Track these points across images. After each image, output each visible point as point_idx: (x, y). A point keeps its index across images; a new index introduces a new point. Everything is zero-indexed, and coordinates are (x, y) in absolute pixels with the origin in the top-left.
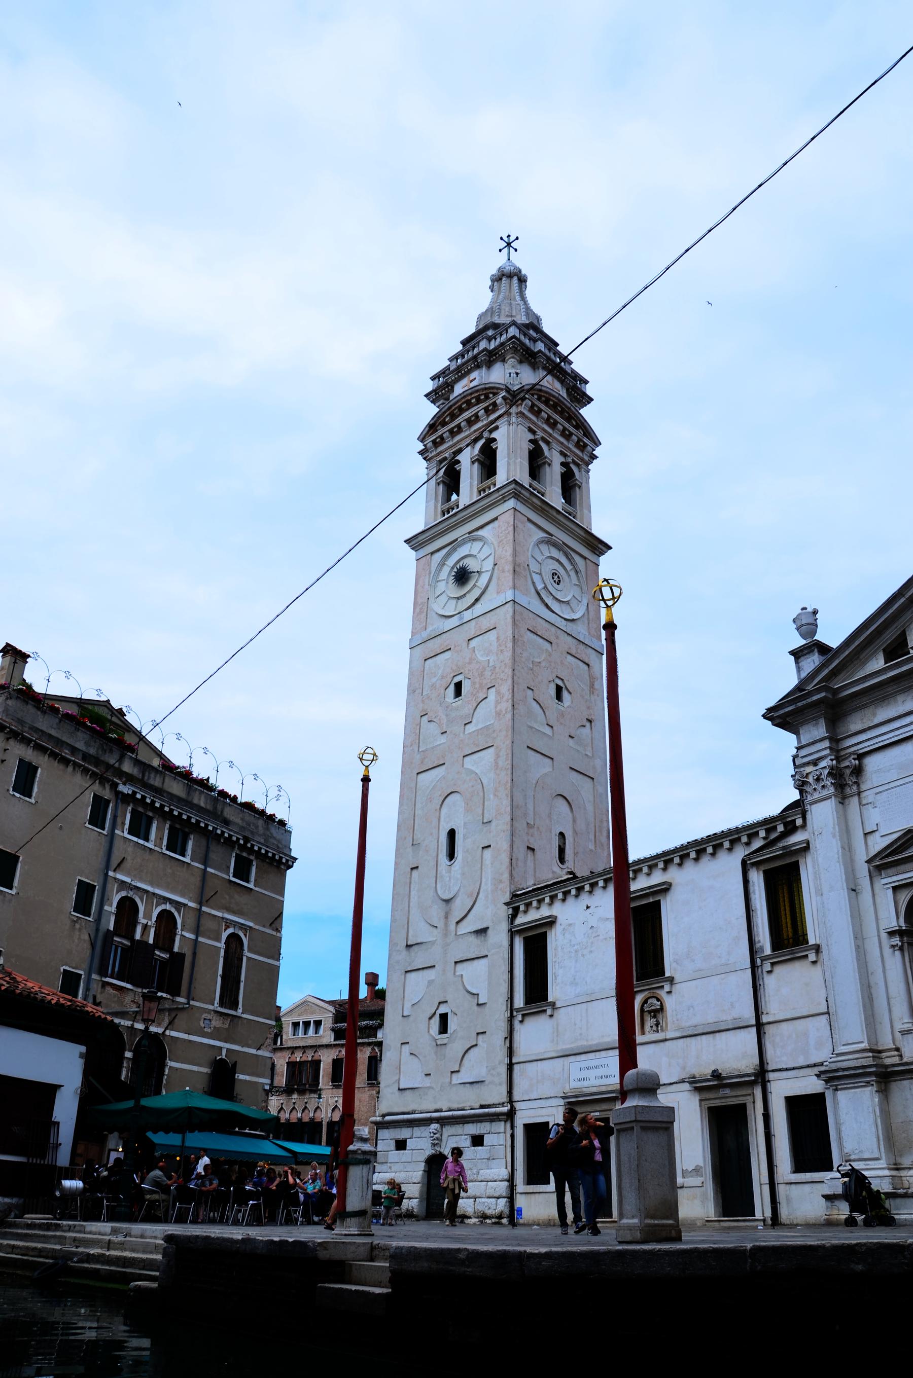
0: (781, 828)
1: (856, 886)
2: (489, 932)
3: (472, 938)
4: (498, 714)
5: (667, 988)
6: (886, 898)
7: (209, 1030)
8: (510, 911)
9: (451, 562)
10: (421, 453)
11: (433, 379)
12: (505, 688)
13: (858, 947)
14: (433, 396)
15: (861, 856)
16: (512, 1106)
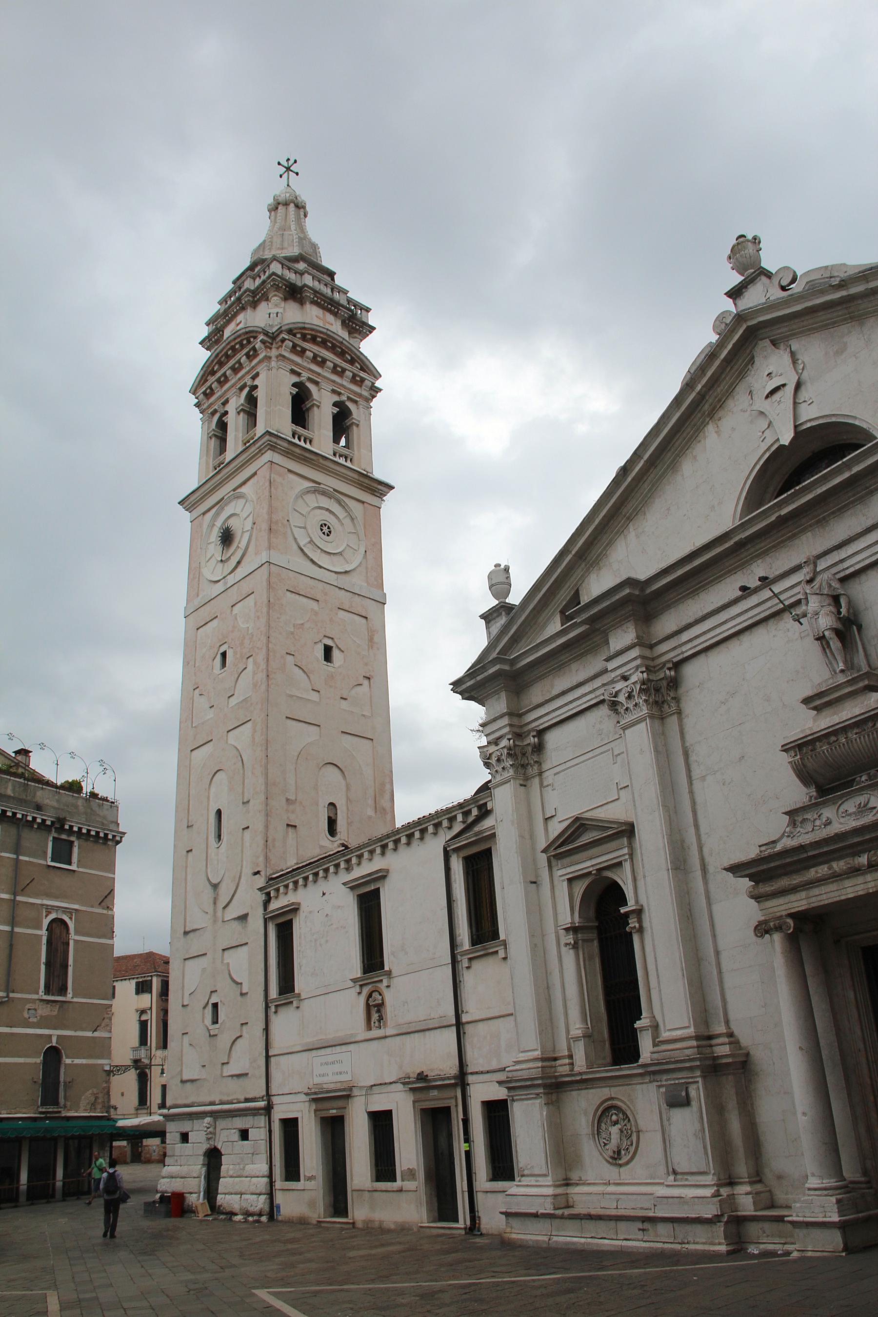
0: (475, 812)
1: (537, 877)
2: (249, 918)
3: (235, 924)
4: (255, 685)
6: (562, 889)
7: (35, 1020)
8: (264, 897)
9: (219, 523)
10: (198, 405)
11: (208, 324)
12: (261, 657)
14: (208, 342)
16: (269, 1101)
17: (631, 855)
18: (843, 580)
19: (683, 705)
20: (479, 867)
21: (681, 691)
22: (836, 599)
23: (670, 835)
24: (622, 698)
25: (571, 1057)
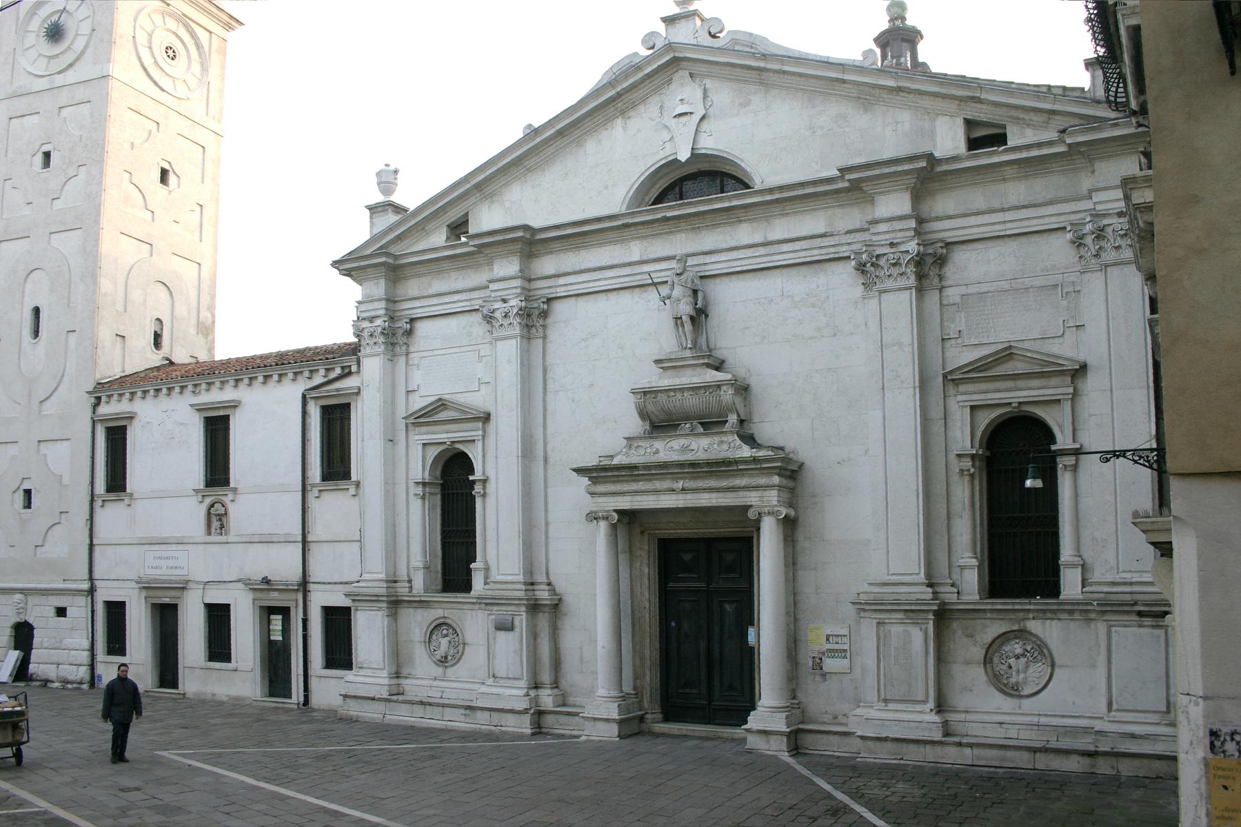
1: (394, 435)
5: (230, 496)
6: (417, 452)
13: (387, 491)
15: (401, 412)
17: (484, 437)
18: (702, 277)
19: (548, 332)
20: (336, 420)
21: (549, 321)
22: (695, 292)
23: (523, 432)
24: (498, 315)
25: (410, 581)
